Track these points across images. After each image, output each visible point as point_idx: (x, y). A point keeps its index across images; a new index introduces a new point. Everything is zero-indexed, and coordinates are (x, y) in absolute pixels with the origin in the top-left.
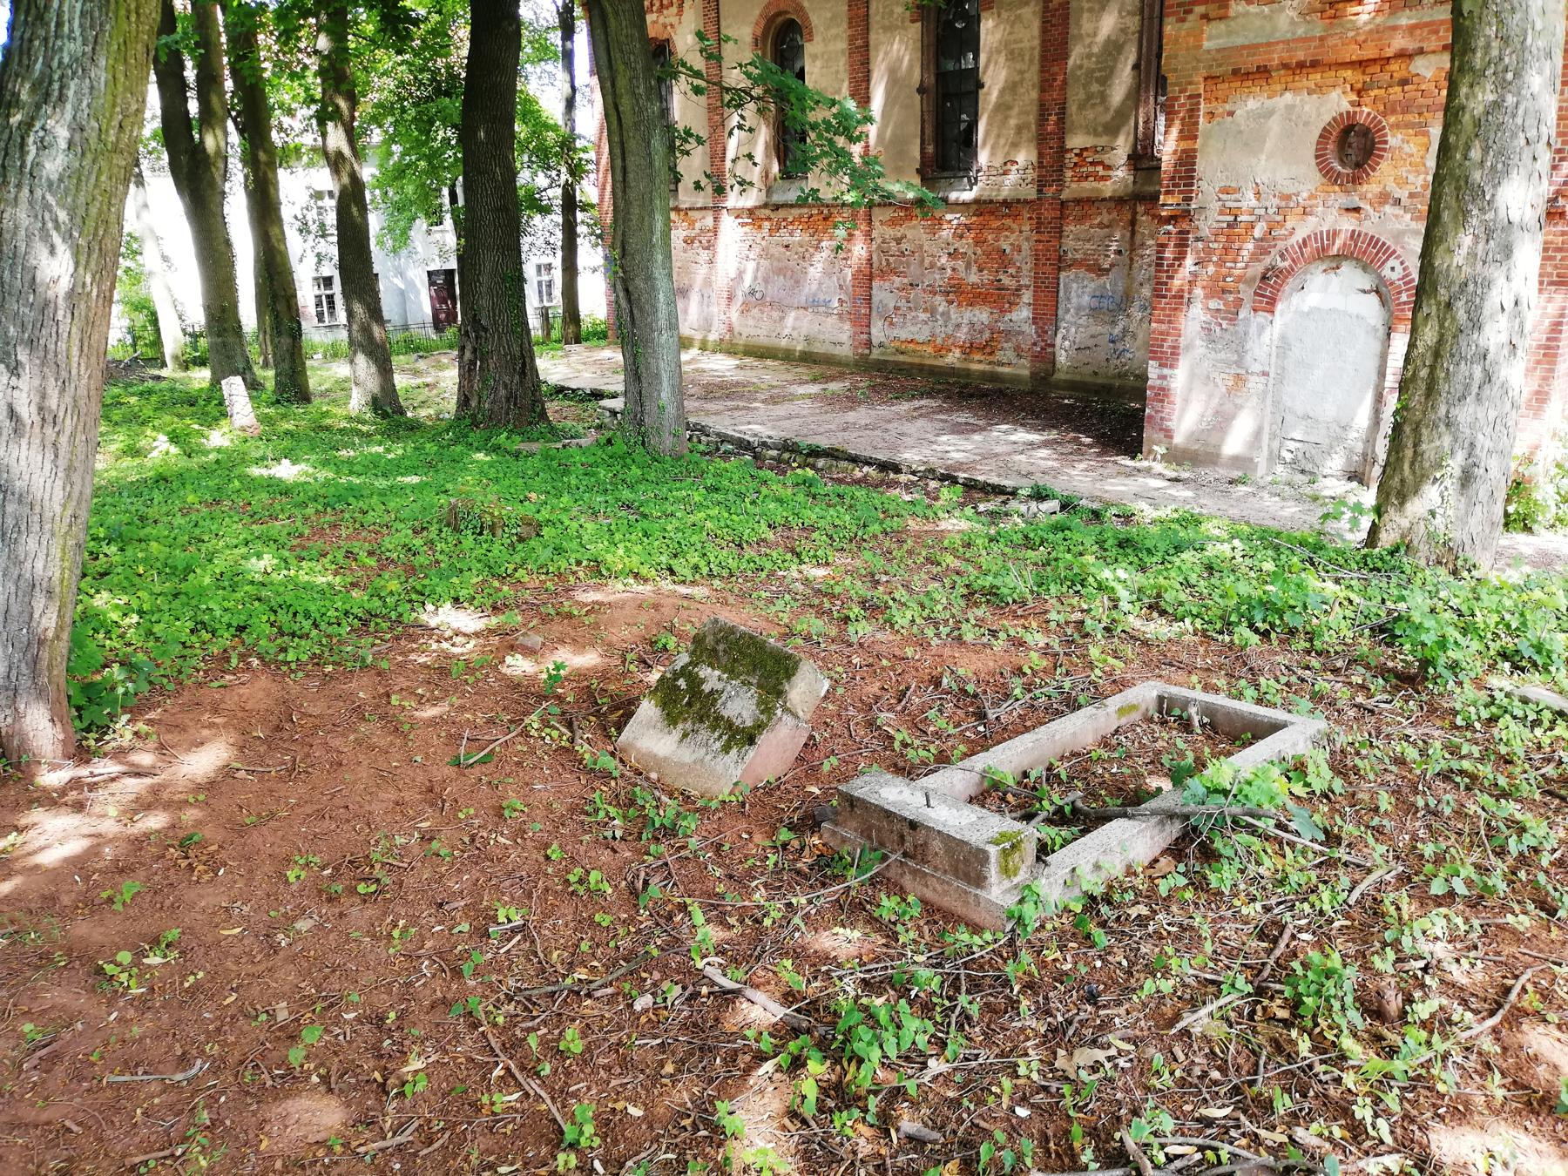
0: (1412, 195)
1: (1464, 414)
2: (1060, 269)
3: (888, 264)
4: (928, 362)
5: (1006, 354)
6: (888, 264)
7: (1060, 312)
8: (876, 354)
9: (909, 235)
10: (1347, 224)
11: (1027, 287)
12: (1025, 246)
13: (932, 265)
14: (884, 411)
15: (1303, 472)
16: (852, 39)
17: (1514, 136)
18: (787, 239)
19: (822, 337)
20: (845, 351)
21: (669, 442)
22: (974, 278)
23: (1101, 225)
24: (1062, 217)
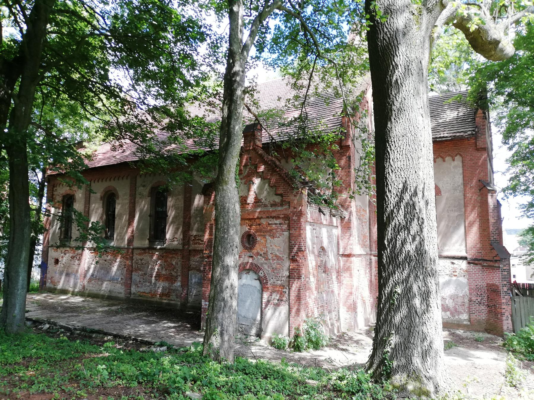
0: (264, 253)
1: (220, 316)
2: (189, 270)
3: (138, 267)
4: (149, 299)
5: (173, 297)
6: (138, 267)
7: (189, 284)
8: (132, 297)
9: (145, 258)
10: (251, 260)
11: (180, 275)
12: (179, 263)
14: (126, 316)
15: (245, 334)
16: (131, 200)
17: (227, 245)
18: (106, 258)
20: (122, 296)
21: (15, 328)
24: (190, 255)
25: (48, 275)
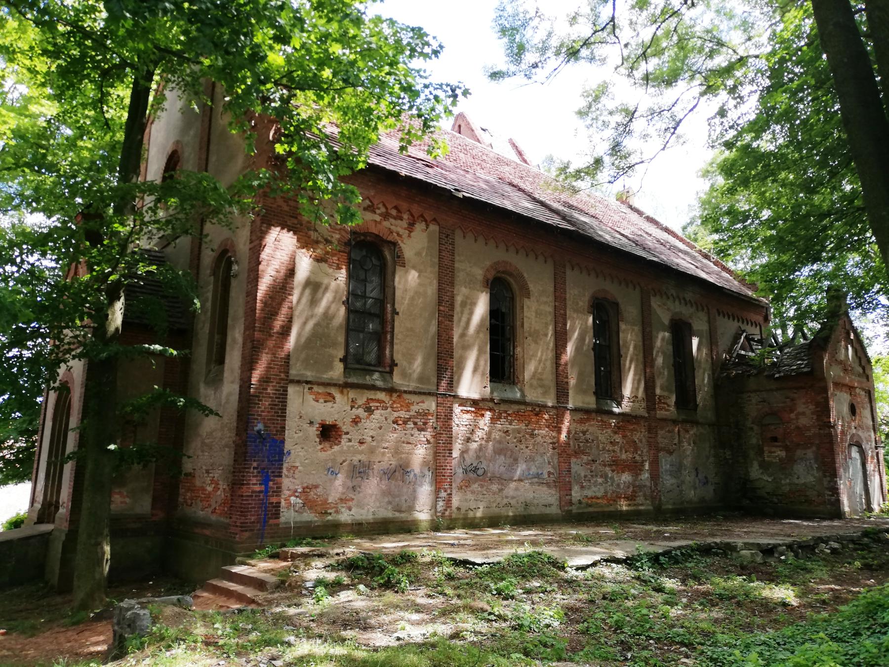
4: (606, 509)
8: (575, 509)
12: (644, 440)
13: (604, 449)
19: (536, 502)
20: (554, 510)
22: (624, 456)
23: (669, 431)
25: (287, 483)
